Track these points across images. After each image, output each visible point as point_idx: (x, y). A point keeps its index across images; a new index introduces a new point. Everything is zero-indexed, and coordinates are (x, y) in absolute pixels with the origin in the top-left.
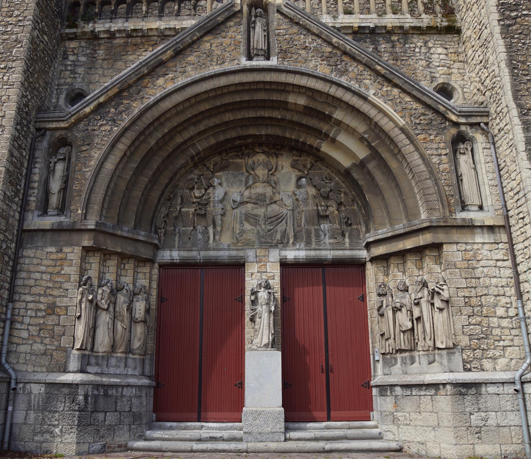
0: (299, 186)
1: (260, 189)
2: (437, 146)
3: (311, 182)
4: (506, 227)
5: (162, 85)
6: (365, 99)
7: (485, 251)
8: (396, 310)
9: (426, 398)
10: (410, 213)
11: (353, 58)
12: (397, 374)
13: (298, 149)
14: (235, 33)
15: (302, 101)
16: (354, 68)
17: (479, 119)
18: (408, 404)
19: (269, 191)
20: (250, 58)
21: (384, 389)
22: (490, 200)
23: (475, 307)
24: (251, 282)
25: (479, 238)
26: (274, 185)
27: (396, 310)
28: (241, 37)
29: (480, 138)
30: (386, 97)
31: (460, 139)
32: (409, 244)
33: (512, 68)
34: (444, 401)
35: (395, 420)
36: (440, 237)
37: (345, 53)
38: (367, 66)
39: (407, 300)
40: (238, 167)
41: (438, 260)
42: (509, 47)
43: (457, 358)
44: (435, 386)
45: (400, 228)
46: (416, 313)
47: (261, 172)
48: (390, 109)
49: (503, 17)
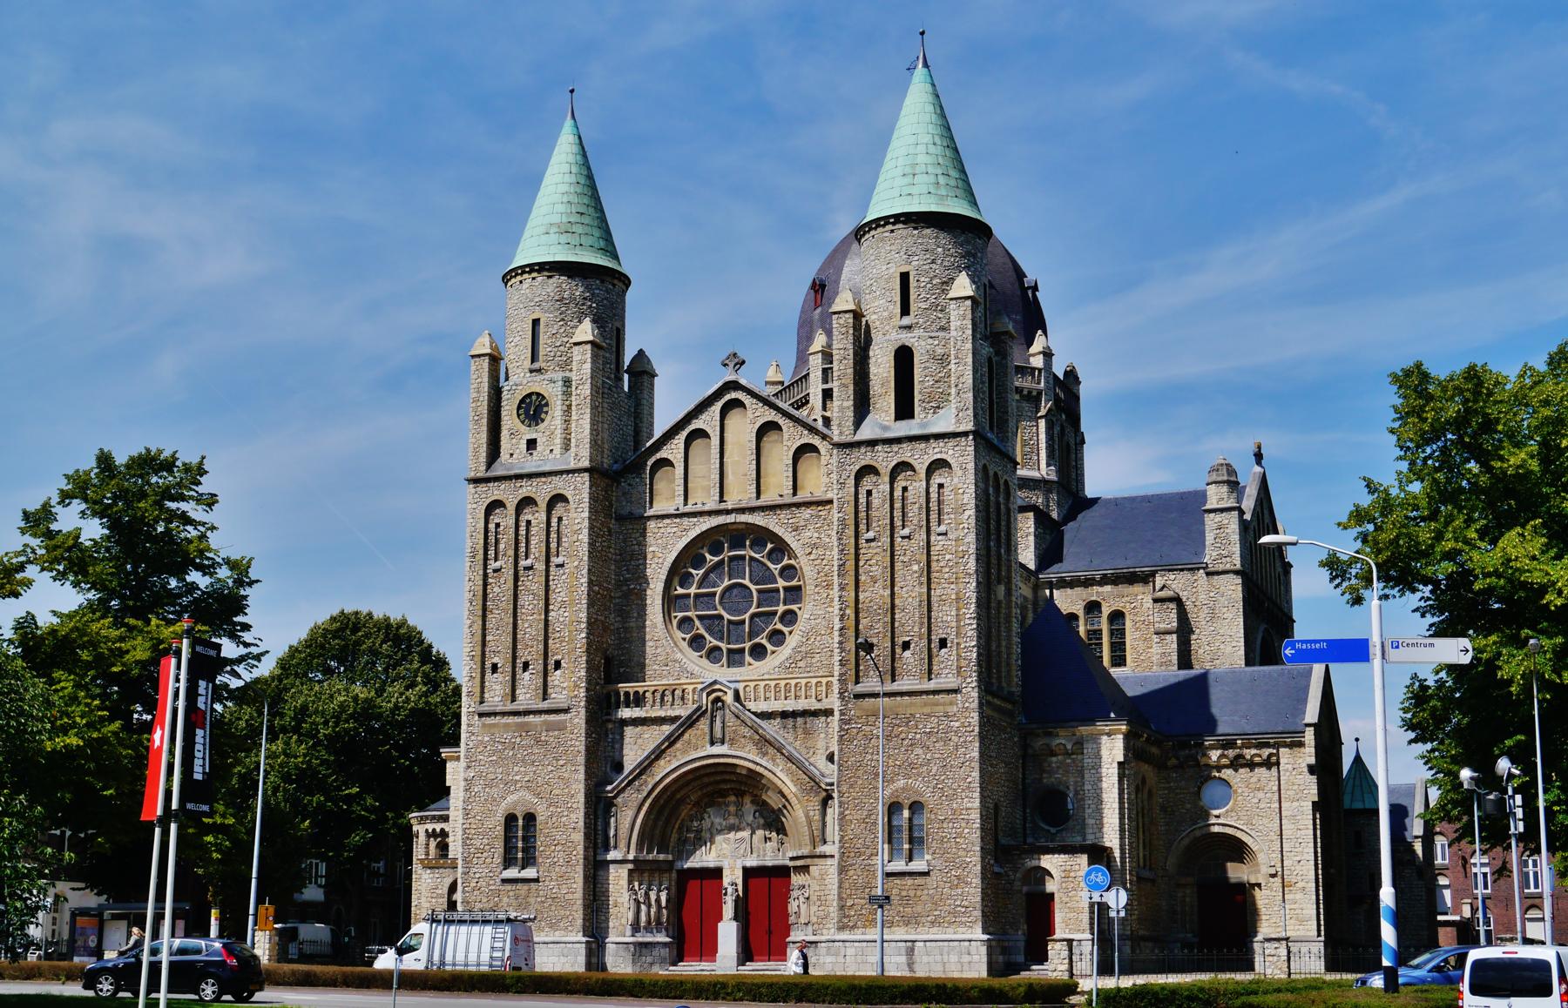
1: (732, 820)
3: (761, 815)
5: (663, 768)
14: (703, 725)
16: (771, 751)
20: (712, 743)
24: (726, 881)
28: (707, 729)
30: (789, 773)
36: (808, 861)
40: (719, 805)
49: (841, 729)
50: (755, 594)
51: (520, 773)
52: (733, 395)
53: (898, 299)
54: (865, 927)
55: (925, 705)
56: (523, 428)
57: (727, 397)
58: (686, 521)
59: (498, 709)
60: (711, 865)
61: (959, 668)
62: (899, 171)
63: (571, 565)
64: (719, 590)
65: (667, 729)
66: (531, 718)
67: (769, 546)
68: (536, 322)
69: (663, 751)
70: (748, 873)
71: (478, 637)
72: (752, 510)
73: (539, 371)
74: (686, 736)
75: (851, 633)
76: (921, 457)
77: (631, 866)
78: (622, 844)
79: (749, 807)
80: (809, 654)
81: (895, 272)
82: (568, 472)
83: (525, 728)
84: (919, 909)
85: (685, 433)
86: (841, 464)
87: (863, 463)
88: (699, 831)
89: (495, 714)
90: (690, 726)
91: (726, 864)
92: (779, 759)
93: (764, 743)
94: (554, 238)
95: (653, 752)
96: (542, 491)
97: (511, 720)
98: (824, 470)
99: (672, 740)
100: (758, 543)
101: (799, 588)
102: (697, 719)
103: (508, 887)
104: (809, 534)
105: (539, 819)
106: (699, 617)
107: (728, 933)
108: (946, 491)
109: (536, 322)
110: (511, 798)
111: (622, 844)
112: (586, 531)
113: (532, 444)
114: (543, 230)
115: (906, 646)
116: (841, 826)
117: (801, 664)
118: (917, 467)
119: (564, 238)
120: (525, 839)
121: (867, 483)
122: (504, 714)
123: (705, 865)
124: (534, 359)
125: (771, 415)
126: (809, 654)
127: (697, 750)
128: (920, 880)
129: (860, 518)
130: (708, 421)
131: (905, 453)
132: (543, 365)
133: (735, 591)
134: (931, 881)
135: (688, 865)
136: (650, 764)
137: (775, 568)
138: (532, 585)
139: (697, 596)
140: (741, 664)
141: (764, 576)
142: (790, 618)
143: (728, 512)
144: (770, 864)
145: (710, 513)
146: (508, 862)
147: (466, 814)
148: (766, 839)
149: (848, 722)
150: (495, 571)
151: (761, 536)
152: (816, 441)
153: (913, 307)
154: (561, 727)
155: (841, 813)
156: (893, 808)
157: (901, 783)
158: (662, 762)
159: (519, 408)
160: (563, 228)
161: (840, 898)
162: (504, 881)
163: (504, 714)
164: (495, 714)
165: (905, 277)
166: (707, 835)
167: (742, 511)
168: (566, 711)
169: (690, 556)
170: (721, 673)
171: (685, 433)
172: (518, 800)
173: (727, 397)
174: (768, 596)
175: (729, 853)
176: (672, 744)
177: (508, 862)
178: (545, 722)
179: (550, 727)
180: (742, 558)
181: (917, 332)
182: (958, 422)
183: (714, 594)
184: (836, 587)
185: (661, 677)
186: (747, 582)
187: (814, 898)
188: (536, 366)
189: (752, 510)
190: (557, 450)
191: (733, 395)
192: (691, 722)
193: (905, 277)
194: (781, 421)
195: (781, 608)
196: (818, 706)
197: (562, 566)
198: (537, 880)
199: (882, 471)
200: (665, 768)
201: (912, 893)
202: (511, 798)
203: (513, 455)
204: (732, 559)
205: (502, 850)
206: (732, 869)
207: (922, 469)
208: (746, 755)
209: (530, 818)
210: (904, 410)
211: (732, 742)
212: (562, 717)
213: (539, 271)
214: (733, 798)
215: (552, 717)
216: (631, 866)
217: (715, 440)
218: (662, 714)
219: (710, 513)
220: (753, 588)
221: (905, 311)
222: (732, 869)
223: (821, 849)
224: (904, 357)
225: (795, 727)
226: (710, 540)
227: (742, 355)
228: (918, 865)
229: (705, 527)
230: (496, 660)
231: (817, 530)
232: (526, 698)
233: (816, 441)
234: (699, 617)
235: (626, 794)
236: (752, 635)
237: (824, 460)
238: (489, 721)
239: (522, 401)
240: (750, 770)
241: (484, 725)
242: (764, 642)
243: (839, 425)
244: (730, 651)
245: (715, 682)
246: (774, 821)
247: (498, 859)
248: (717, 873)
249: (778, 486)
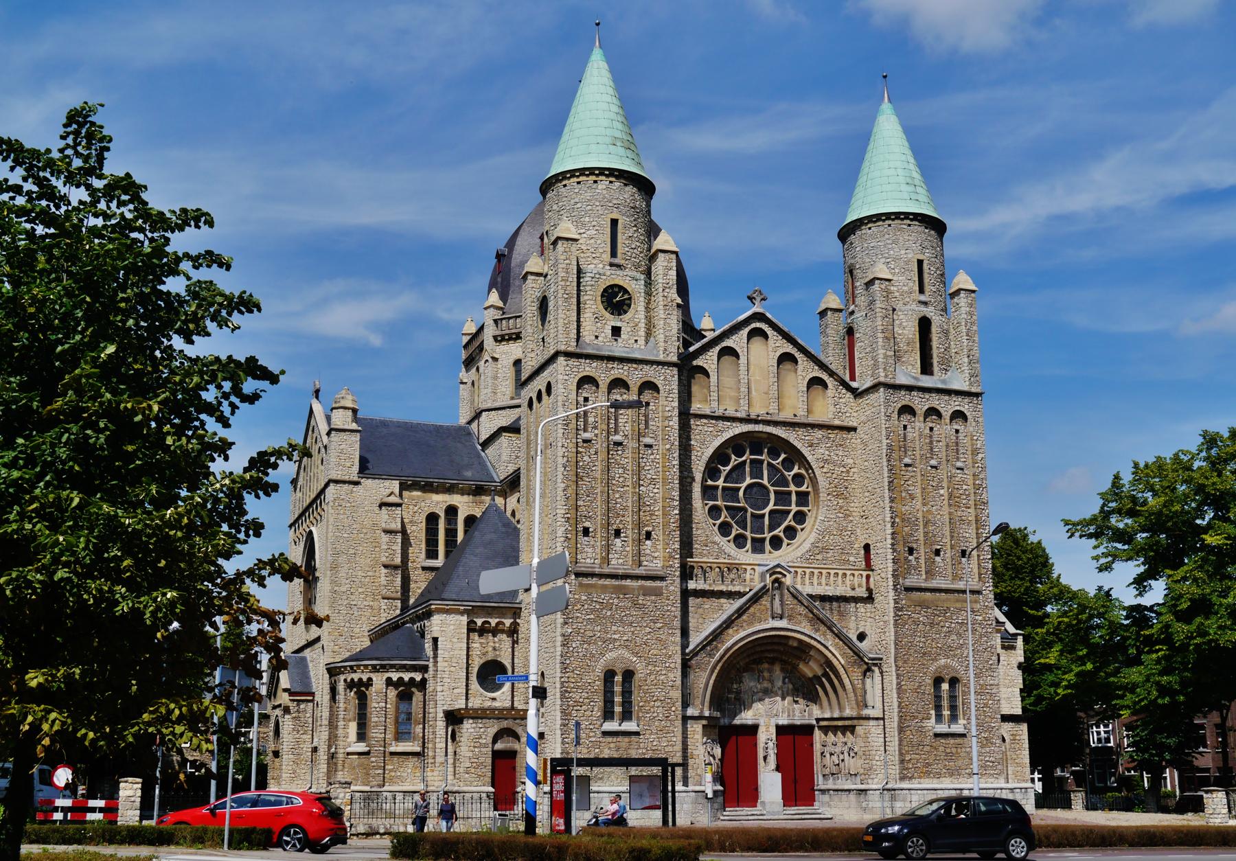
0: (784, 683)
1: (766, 684)
2: (857, 674)
3: (790, 681)
4: (883, 719)
6: (827, 648)
7: (873, 730)
8: (831, 754)
9: (844, 795)
10: (841, 708)
11: (822, 622)
12: (830, 784)
13: (783, 662)
14: (765, 601)
15: (795, 644)
16: (823, 628)
17: (878, 662)
18: (836, 798)
19: (769, 685)
21: (823, 791)
22: (879, 705)
23: (867, 755)
25: (872, 723)
26: (771, 681)
27: (831, 754)
28: (769, 605)
29: (876, 669)
30: (836, 645)
31: (869, 669)
32: (840, 723)
33: (896, 644)
34: (852, 796)
35: (829, 806)
36: (855, 722)
37: (818, 619)
38: (830, 629)
39: (838, 749)
40: (753, 670)
41: (853, 733)
42: (896, 632)
43: (858, 778)
44: (849, 791)
45: (836, 715)
46: (841, 757)
47: (766, 674)
48: (838, 655)
50: (772, 496)
51: (617, 632)
52: (758, 325)
53: (916, 279)
54: (920, 777)
55: (957, 601)
56: (607, 315)
57: (753, 325)
58: (720, 423)
59: (597, 570)
60: (750, 722)
61: (980, 574)
62: (902, 179)
63: (662, 447)
64: (744, 485)
65: (739, 603)
66: (628, 582)
67: (783, 456)
68: (614, 222)
69: (733, 622)
70: (780, 729)
71: (572, 502)
72: (776, 424)
73: (619, 266)
74: (752, 610)
76: (947, 406)
77: (705, 722)
78: (698, 702)
79: (778, 673)
80: (824, 550)
81: (913, 256)
82: (658, 363)
83: (623, 591)
84: (959, 763)
85: (718, 348)
86: (887, 401)
87: (904, 403)
88: (738, 692)
89: (592, 575)
90: (756, 602)
91: (762, 722)
92: (829, 635)
93: (818, 620)
94: (622, 151)
95: (724, 622)
96: (635, 376)
97: (608, 582)
98: (830, 401)
99: (740, 612)
101: (807, 494)
102: (761, 597)
103: (610, 739)
104: (821, 451)
105: (637, 677)
106: (727, 508)
107: (770, 783)
108: (961, 436)
109: (614, 222)
110: (610, 656)
111: (698, 702)
112: (676, 419)
113: (616, 331)
114: (608, 140)
116: (898, 694)
117: (819, 557)
118: (944, 414)
119: (629, 153)
120: (623, 693)
121: (906, 418)
122: (601, 576)
123: (744, 722)
124: (614, 254)
125: (789, 348)
126: (824, 550)
127: (763, 624)
128: (959, 740)
129: (898, 447)
130: (738, 341)
131: (935, 401)
132: (622, 262)
133: (755, 489)
135: (737, 721)
136: (721, 633)
137: (789, 475)
139: (724, 489)
140: (762, 551)
142: (800, 517)
143: (756, 422)
144: (798, 723)
145: (741, 420)
146: (608, 714)
147: (565, 668)
148: (796, 702)
149: (900, 609)
150: (585, 441)
151: (778, 446)
152: (825, 376)
153: (927, 288)
154: (658, 593)
155: (898, 684)
156: (938, 681)
157: (943, 662)
158: (730, 631)
159: (602, 296)
160: (627, 144)
161: (901, 754)
162: (605, 734)
163: (601, 576)
164: (592, 575)
165: (920, 262)
166: (745, 696)
167: (768, 423)
168: (662, 579)
169: (720, 456)
170: (771, 558)
171: (718, 348)
172: (615, 656)
173: (753, 325)
175: (767, 715)
176: (740, 616)
177: (608, 714)
178: (642, 587)
179: (647, 592)
180: (762, 462)
181: (931, 308)
182: (971, 384)
183: (738, 489)
184: (887, 500)
185: (702, 555)
186: (765, 482)
187: (860, 753)
188: (616, 261)
189: (776, 424)
190: (642, 341)
191: (758, 325)
192: (756, 598)
193: (920, 262)
194: (798, 355)
196: (852, 594)
197: (650, 446)
198: (637, 734)
199: (918, 412)
200: (735, 637)
201: (954, 750)
202: (610, 656)
204: (752, 461)
205: (601, 704)
206: (768, 727)
207: (947, 415)
208: (802, 629)
209: (629, 675)
210: (926, 368)
211: (790, 618)
212: (658, 584)
213: (617, 177)
214: (766, 666)
215: (648, 583)
216: (705, 722)
218: (724, 588)
219: (741, 420)
220: (771, 489)
221: (921, 291)
222: (768, 727)
223: (865, 712)
224: (925, 325)
225: (831, 609)
226: (736, 445)
227: (765, 293)
228: (957, 728)
229: (737, 431)
230: (587, 524)
231: (828, 449)
232: (618, 563)
233: (825, 376)
234: (727, 508)
235: (698, 658)
236: (771, 529)
237: (831, 391)
238: (585, 581)
239: (605, 290)
240: (800, 641)
241: (581, 585)
242: (782, 534)
243: (885, 369)
244: (753, 539)
245: (778, 566)
246: (807, 690)
247: (598, 713)
248: (753, 730)
249: (795, 404)
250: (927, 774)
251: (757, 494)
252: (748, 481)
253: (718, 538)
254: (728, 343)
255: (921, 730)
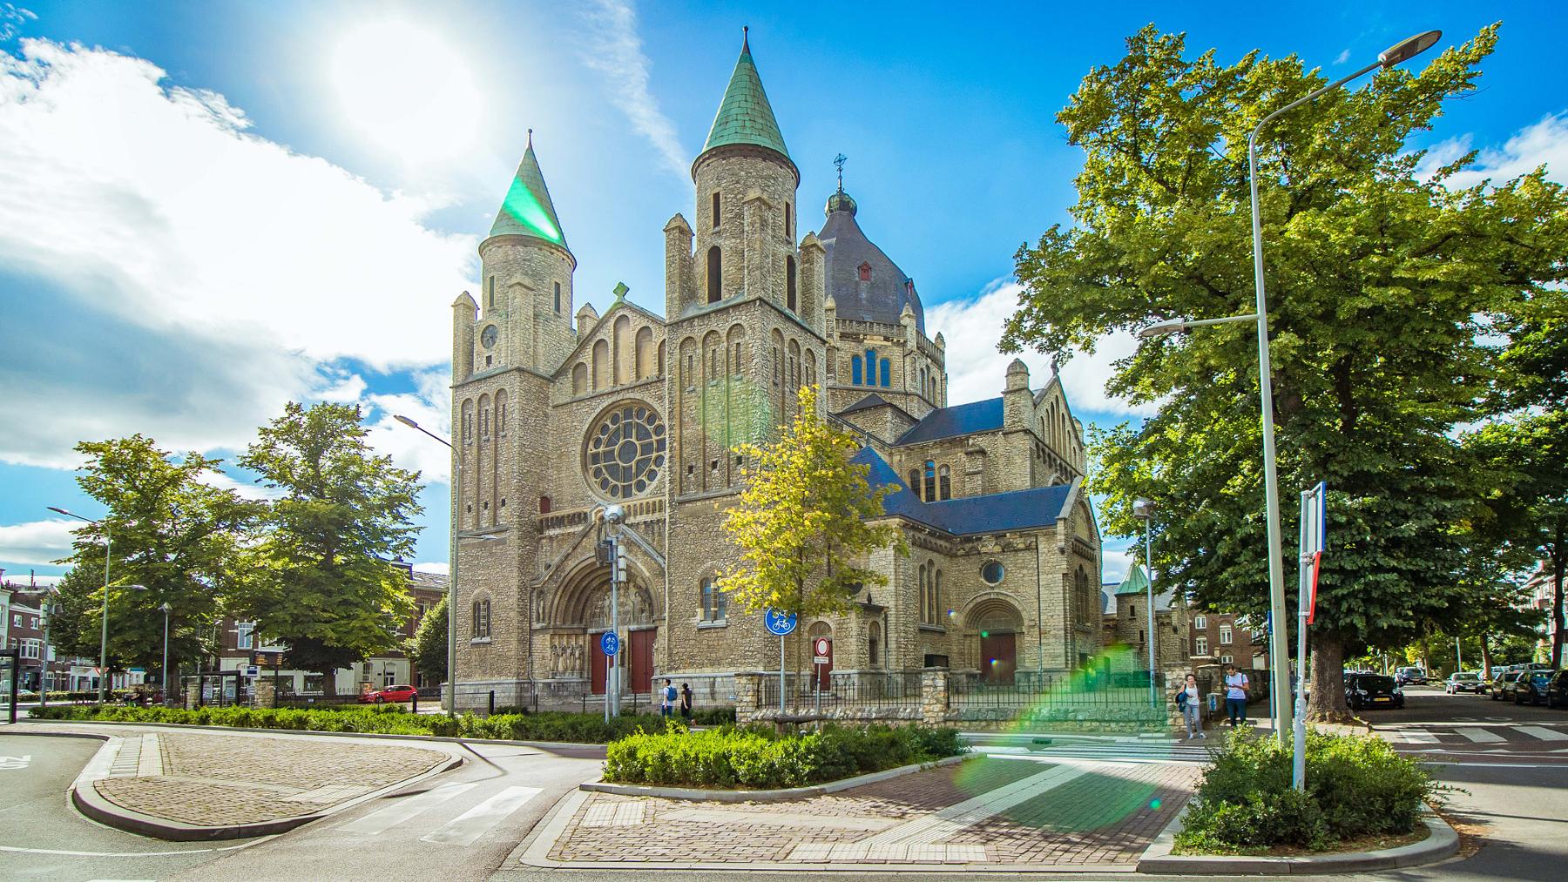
30: (645, 564)
75: (677, 459)
84: (720, 654)
100: (640, 414)
113: (489, 359)
115: (714, 465)
134: (729, 633)
137: (650, 428)
138: (488, 451)
141: (643, 434)
174: (647, 449)
195: (654, 455)
203: (480, 367)
217: (611, 346)
228: (718, 623)
250: (691, 665)
251: (628, 450)
252: (622, 441)
253: (648, 490)
254: (599, 336)
255: (688, 627)
